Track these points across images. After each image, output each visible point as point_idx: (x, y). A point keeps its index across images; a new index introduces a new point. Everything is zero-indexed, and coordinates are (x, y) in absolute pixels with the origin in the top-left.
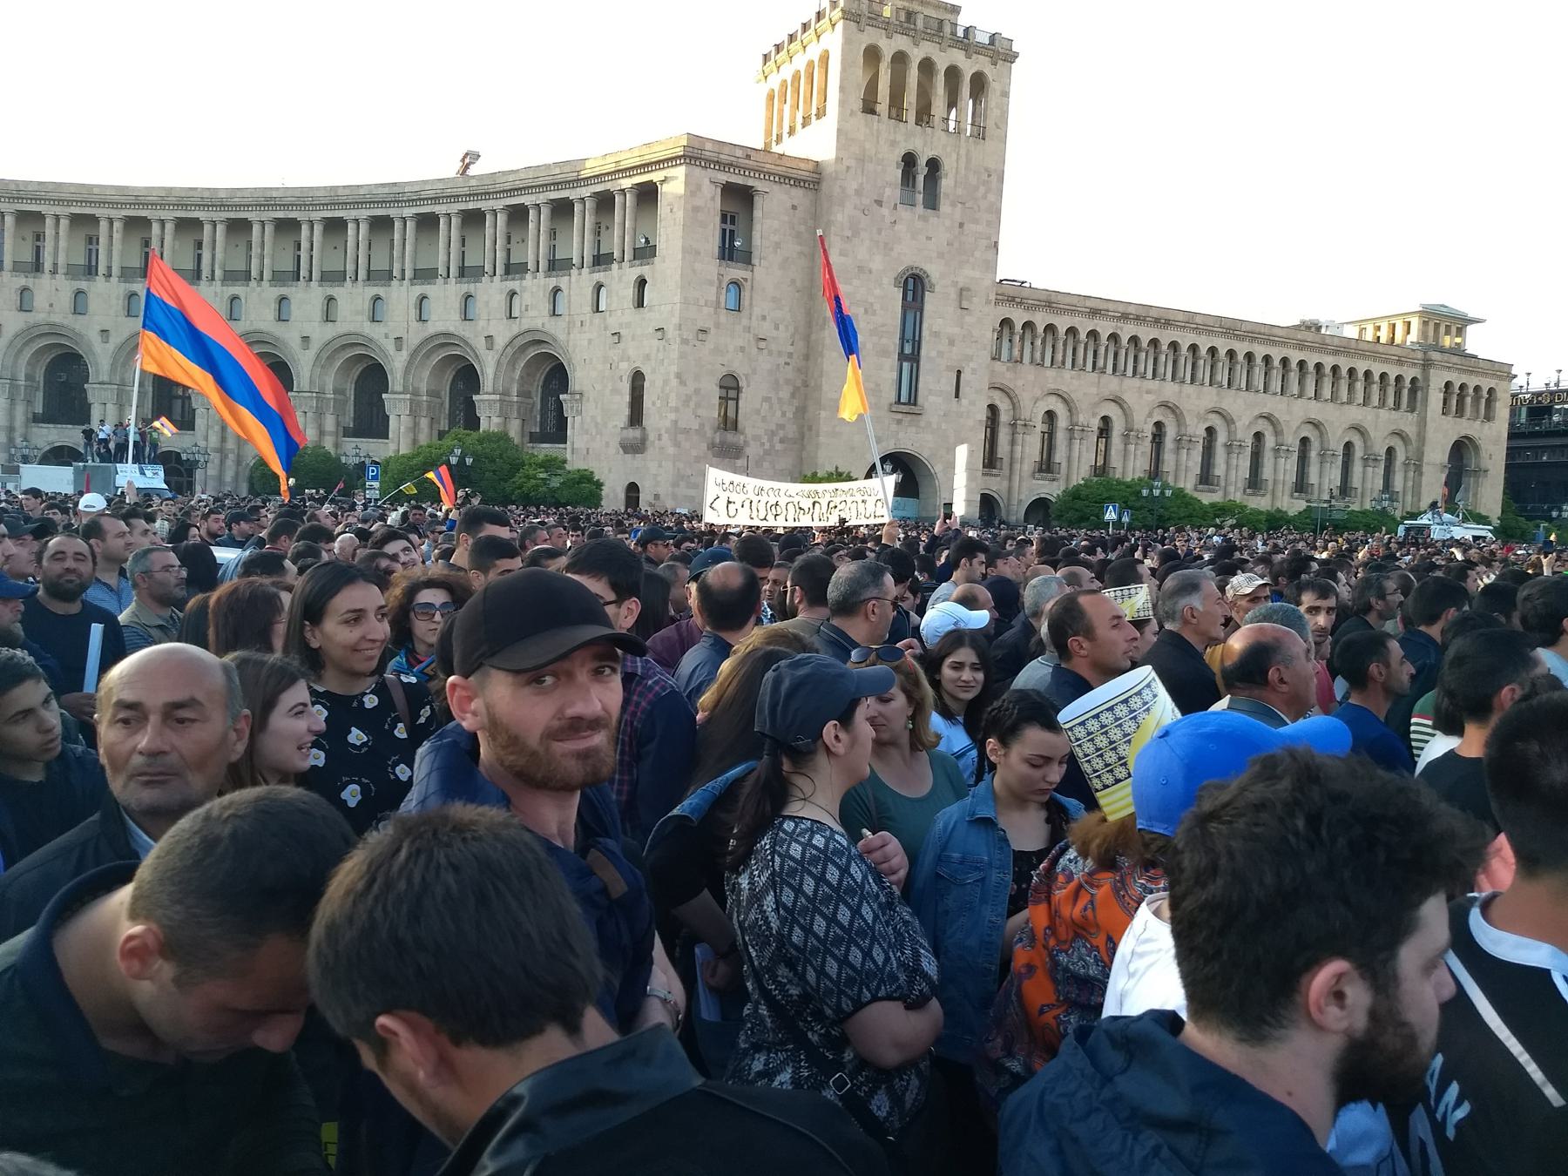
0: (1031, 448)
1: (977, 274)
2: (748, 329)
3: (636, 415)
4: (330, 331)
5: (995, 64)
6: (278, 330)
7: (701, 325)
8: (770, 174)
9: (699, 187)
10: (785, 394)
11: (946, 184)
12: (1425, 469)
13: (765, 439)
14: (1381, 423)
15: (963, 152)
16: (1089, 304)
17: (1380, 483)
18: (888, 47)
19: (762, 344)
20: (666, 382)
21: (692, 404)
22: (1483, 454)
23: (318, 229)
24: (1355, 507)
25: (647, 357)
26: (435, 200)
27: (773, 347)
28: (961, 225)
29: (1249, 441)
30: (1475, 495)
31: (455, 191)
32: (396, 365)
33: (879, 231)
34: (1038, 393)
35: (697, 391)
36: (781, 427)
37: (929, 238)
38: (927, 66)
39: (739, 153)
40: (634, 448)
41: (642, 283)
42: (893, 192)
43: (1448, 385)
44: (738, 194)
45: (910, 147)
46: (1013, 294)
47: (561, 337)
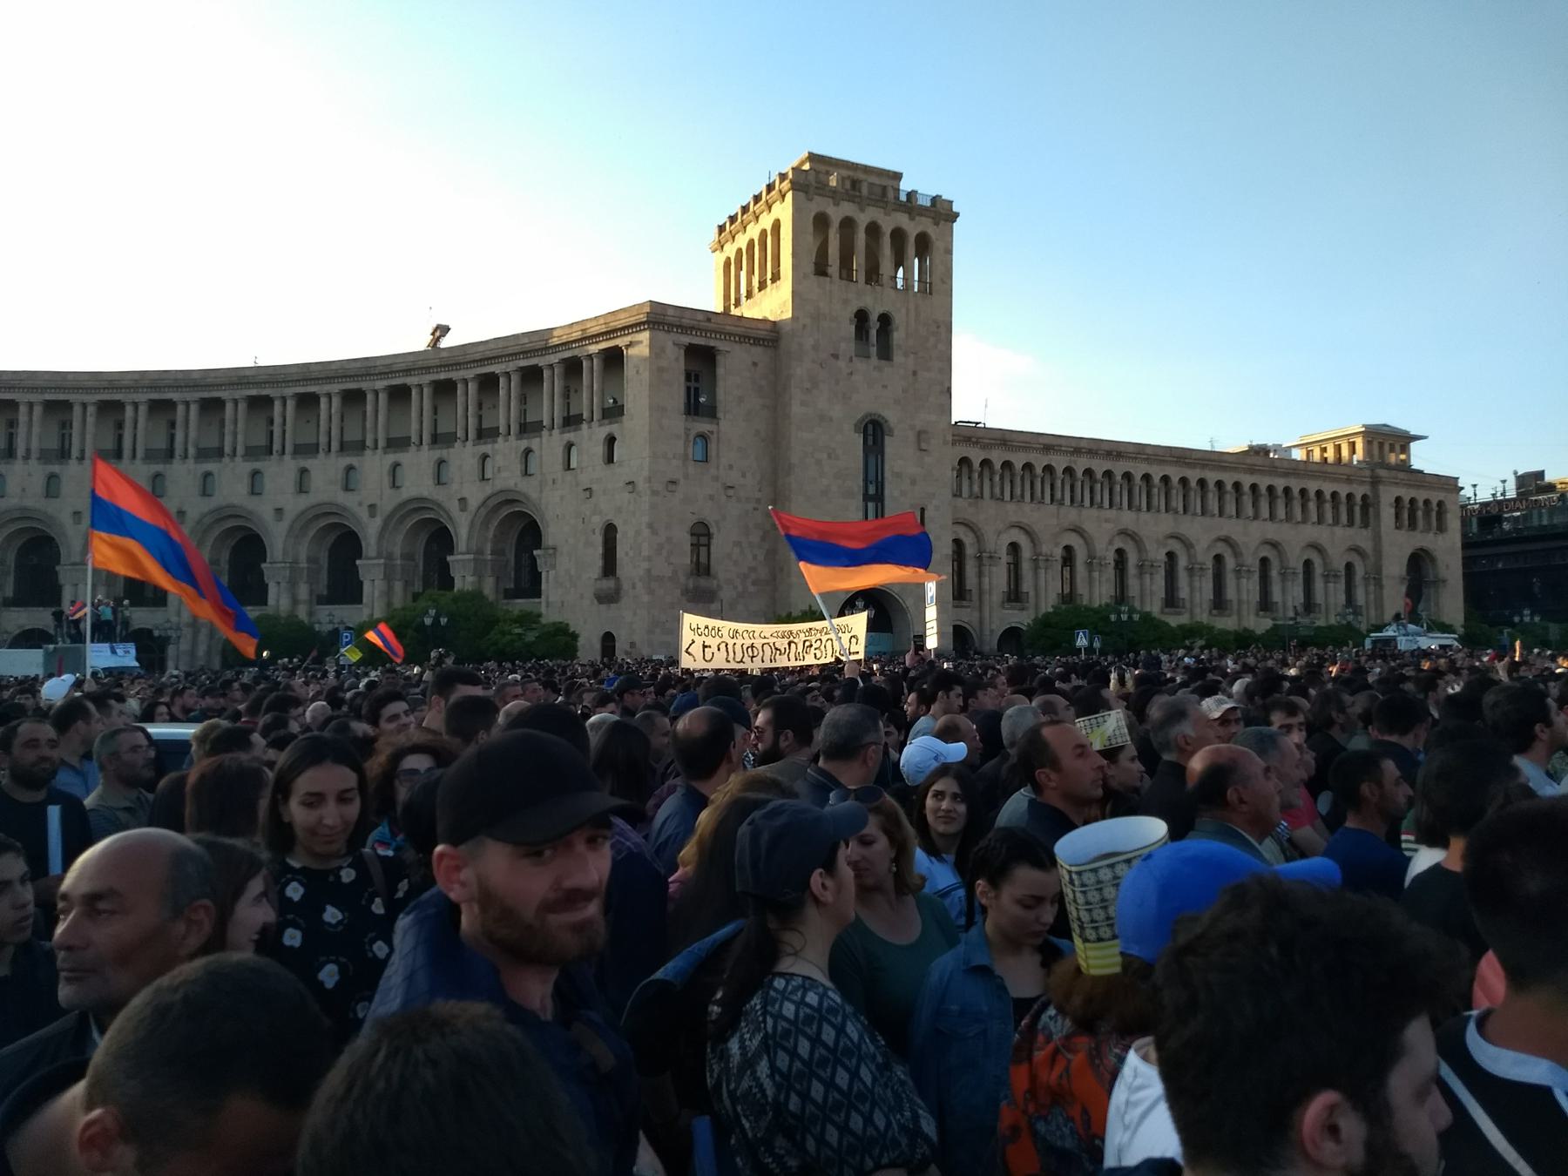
0: (998, 578)
1: (933, 418)
3: (610, 565)
4: (304, 502)
5: (937, 224)
6: (251, 504)
8: (730, 334)
9: (663, 350)
10: (755, 537)
11: (898, 336)
12: (1384, 582)
14: (1338, 540)
16: (1041, 440)
17: (1342, 598)
18: (836, 214)
19: (731, 492)
20: (638, 533)
21: (664, 553)
23: (291, 404)
24: (1321, 623)
25: (619, 510)
26: (408, 371)
28: (915, 373)
29: (1210, 564)
30: (1437, 604)
31: (426, 364)
32: (370, 531)
35: (669, 539)
36: (753, 569)
37: (885, 387)
38: (873, 230)
39: (700, 317)
40: (608, 598)
41: (611, 441)
42: (848, 346)
43: (1398, 500)
44: (698, 349)
46: (973, 434)
47: (534, 495)
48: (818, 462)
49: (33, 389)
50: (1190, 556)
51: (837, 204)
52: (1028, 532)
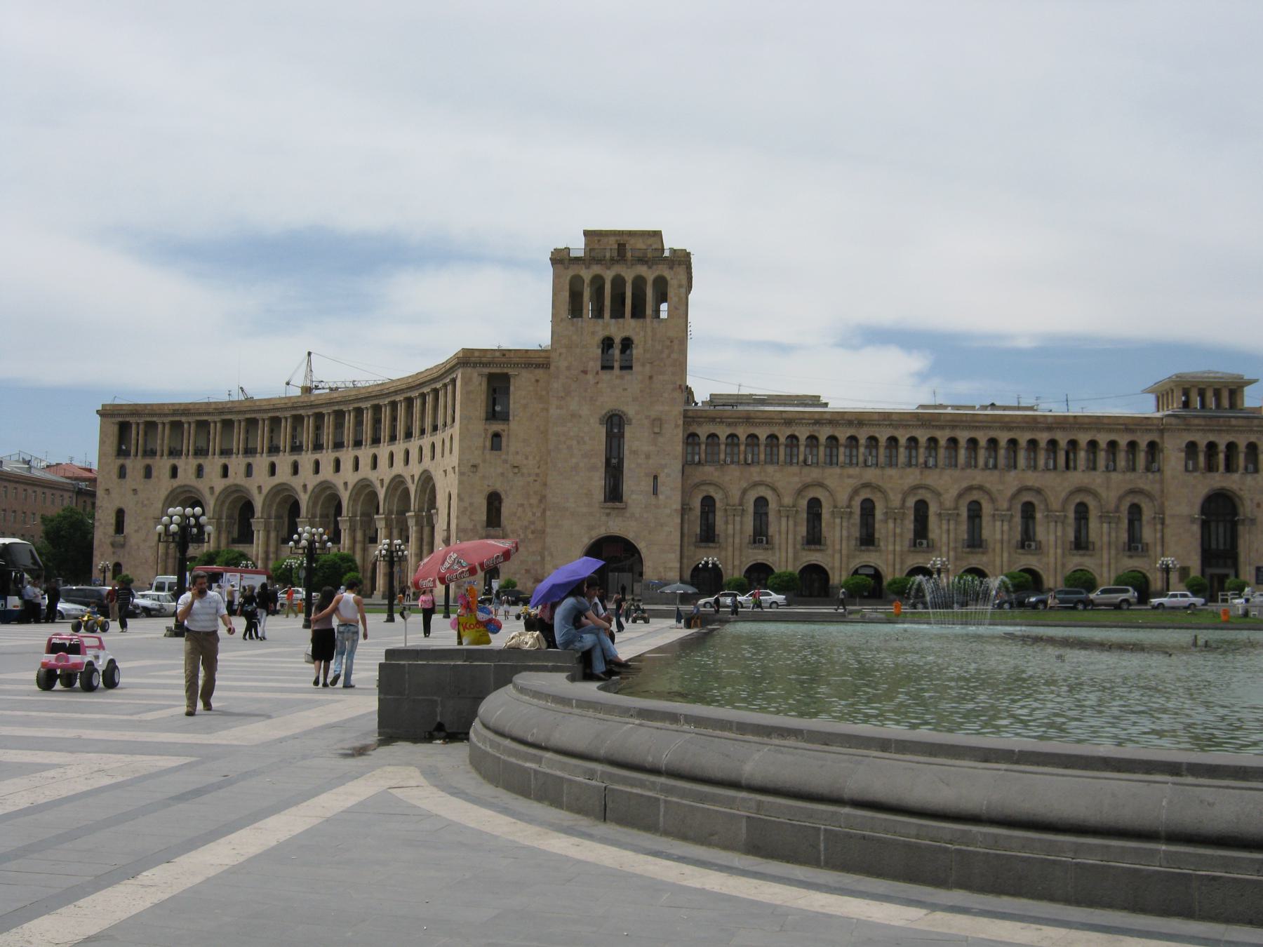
1: (667, 408)
2: (505, 462)
5: (671, 268)
7: (473, 462)
9: (470, 379)
10: (534, 501)
11: (636, 352)
12: (1168, 521)
13: (520, 532)
15: (649, 330)
18: (587, 274)
22: (1247, 503)
27: (525, 471)
28: (651, 377)
33: (586, 391)
34: (745, 485)
35: (471, 504)
36: (533, 523)
37: (625, 390)
39: (497, 354)
44: (494, 379)
45: (607, 333)
48: (570, 447)
49: (240, 412)
50: (941, 504)
51: (588, 268)
52: (774, 490)
